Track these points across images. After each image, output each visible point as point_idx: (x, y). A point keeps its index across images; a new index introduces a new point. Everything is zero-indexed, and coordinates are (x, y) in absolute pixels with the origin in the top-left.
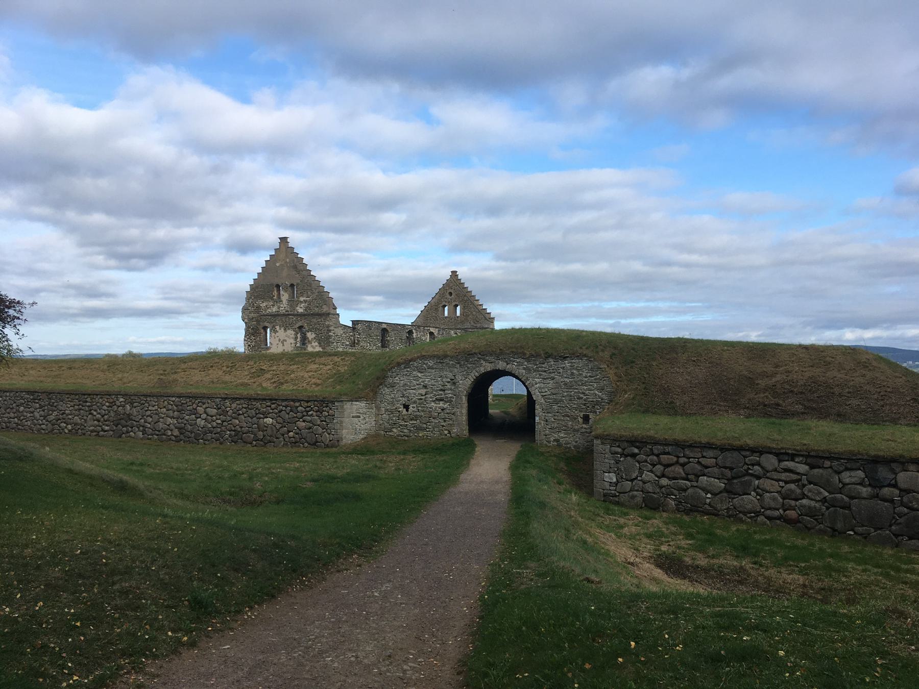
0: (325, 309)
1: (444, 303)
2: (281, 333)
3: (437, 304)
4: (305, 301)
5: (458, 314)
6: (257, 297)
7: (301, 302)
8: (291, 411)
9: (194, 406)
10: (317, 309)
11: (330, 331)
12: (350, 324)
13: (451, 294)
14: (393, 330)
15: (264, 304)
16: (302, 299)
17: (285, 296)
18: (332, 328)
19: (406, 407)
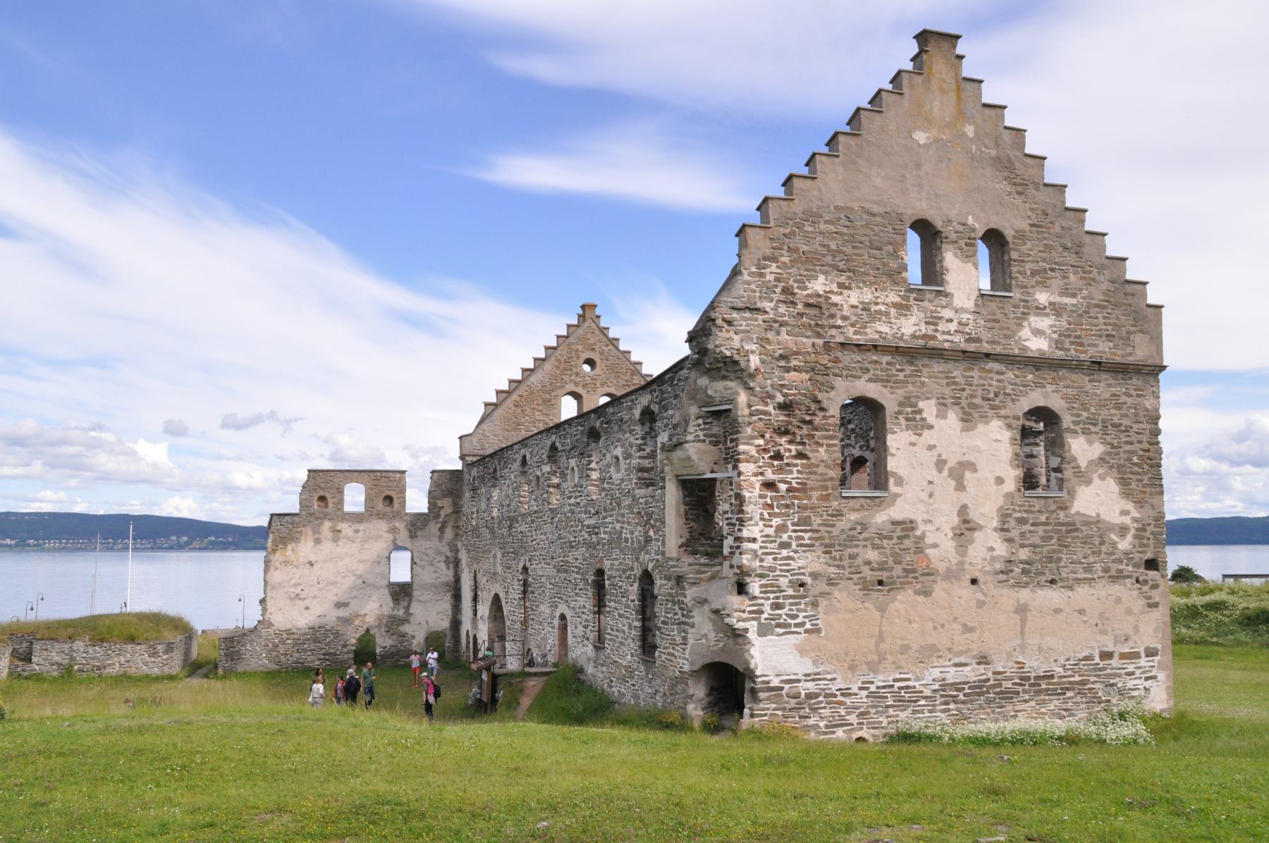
0: (1140, 352)
2: (946, 430)
4: (1057, 310)
6: (810, 263)
7: (1040, 310)
13: (590, 362)
16: (1042, 298)
17: (968, 277)
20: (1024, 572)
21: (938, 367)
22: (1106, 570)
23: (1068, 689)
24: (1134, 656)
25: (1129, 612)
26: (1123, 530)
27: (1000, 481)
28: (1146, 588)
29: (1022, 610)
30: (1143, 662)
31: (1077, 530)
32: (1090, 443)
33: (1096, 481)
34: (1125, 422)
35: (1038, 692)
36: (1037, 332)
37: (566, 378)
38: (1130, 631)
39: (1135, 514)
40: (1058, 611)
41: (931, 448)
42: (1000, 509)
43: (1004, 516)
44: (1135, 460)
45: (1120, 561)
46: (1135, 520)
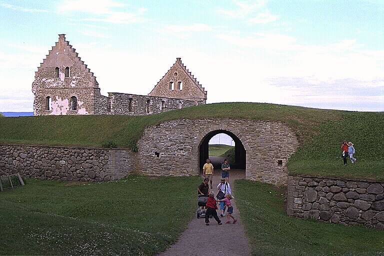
5: (181, 89)
6: (42, 77)
7: (74, 80)
8: (78, 155)
9: (12, 151)
10: (84, 85)
12: (107, 95)
16: (74, 78)
17: (62, 76)
19: (158, 154)
21: (59, 90)
36: (73, 84)
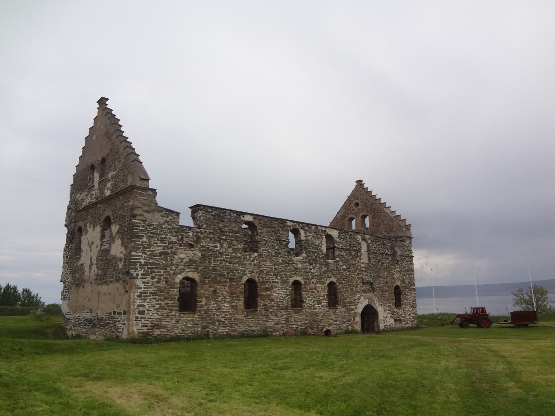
1: (351, 216)
3: (343, 218)
5: (367, 225)
7: (109, 180)
11: (134, 216)
14: (265, 226)
15: (82, 196)
18: (138, 212)
20: (100, 279)
22: (116, 277)
23: (107, 325)
24: (120, 314)
25: (120, 295)
26: (121, 259)
27: (97, 246)
28: (125, 284)
29: (99, 293)
30: (123, 317)
31: (111, 261)
32: (116, 226)
33: (116, 241)
34: (124, 214)
35: (101, 325)
36: (108, 189)
37: (349, 212)
38: (120, 303)
39: (124, 252)
40: (105, 294)
41: (87, 239)
42: (97, 256)
43: (97, 259)
44: (126, 229)
45: (119, 273)
46: (124, 255)
